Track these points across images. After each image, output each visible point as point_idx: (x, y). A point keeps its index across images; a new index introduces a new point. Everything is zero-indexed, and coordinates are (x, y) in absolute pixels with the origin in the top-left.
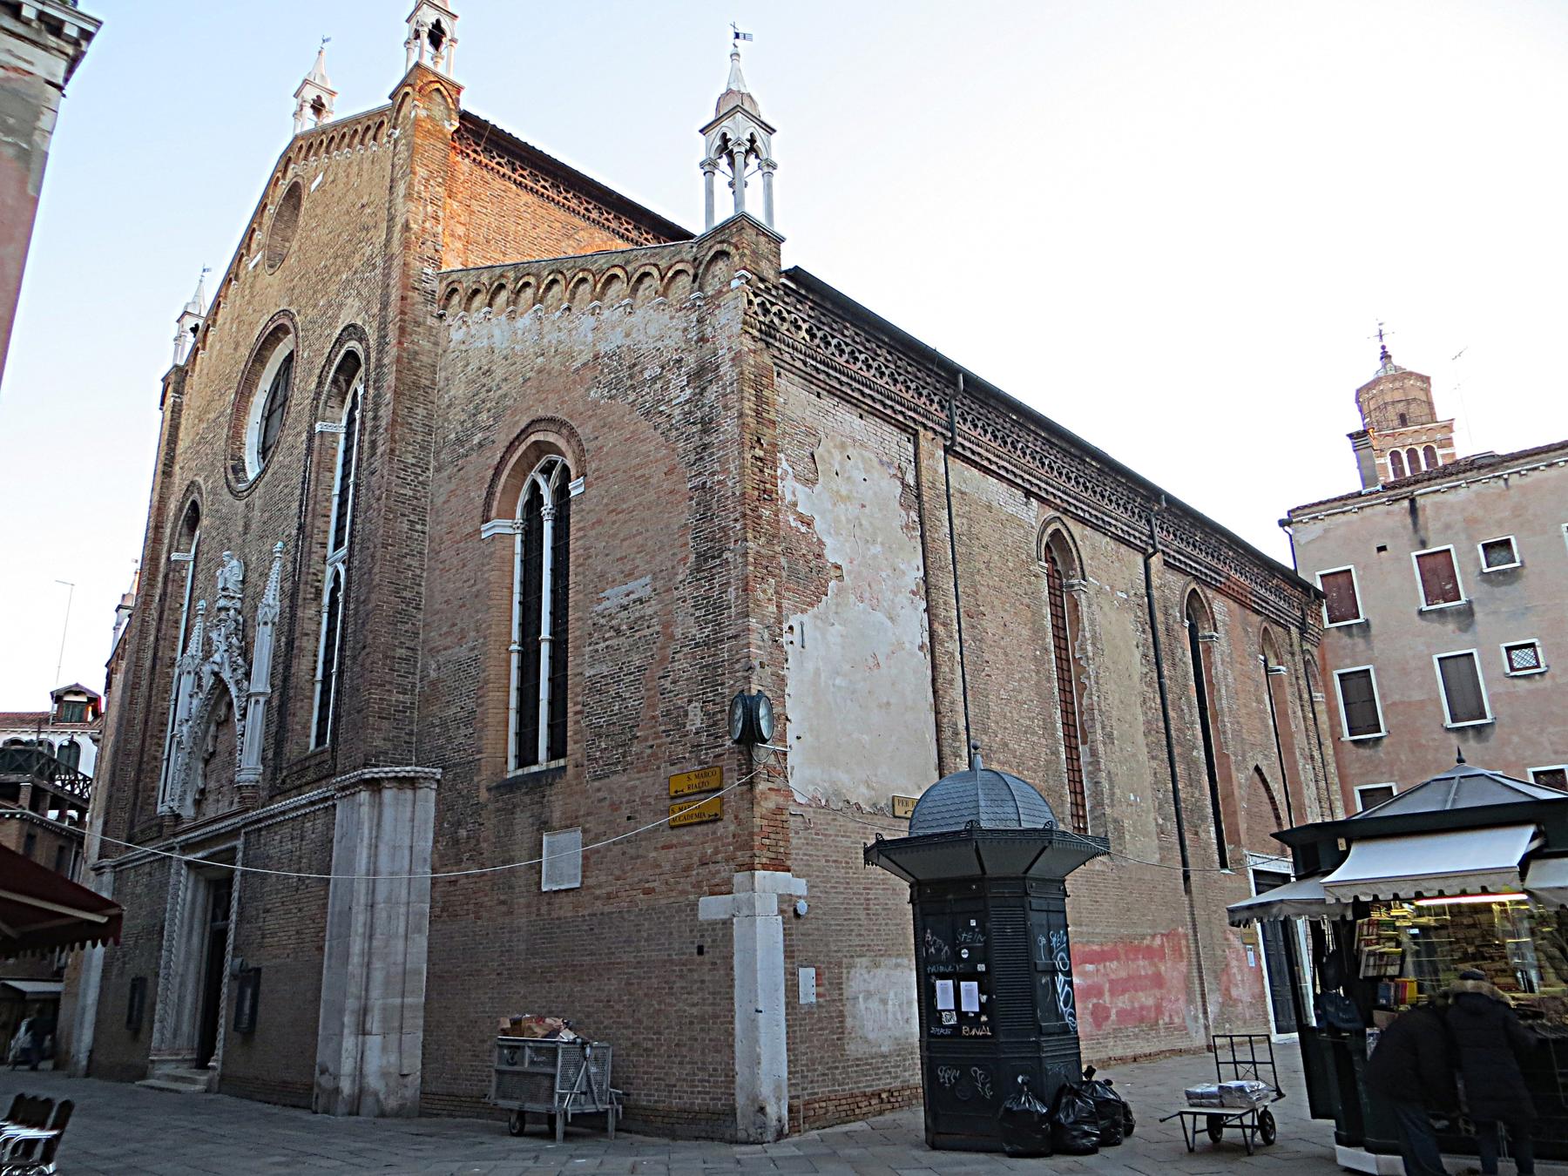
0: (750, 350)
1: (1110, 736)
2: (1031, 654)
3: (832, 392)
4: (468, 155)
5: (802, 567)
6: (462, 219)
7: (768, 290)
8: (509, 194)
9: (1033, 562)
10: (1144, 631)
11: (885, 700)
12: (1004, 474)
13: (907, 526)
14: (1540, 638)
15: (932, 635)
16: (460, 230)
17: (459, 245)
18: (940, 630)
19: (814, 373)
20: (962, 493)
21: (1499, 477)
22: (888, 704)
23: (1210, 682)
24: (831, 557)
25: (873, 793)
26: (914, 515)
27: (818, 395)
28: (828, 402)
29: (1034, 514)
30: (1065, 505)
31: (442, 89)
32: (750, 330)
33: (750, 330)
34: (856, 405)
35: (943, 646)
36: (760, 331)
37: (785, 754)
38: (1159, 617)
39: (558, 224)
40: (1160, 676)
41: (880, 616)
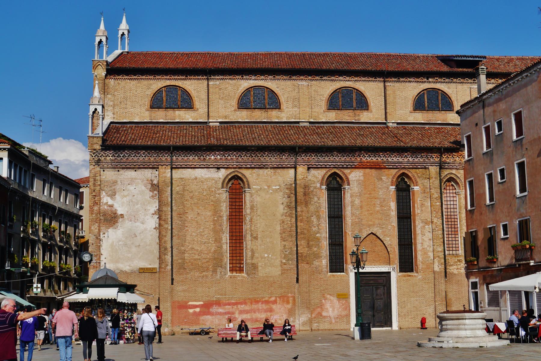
0: (93, 169)
1: (256, 238)
2: (211, 220)
3: (123, 168)
4: (112, 78)
5: (109, 218)
6: (112, 100)
7: (97, 152)
8: (127, 84)
9: (219, 189)
10: (289, 197)
11: (138, 245)
12: (203, 166)
13: (152, 196)
14: (506, 167)
15: (160, 225)
16: (111, 103)
17: (111, 108)
18: (162, 223)
19: (115, 166)
20: (181, 178)
21: (500, 90)
22: (139, 245)
23: (344, 205)
24: (119, 213)
25: (131, 268)
26: (156, 192)
27: (118, 171)
28: (122, 171)
29: (223, 173)
30: (239, 166)
31: (100, 64)
32: (92, 164)
33: (92, 164)
34: (133, 168)
35: (163, 227)
36: (95, 163)
37: (100, 263)
38: (300, 191)
39: (145, 86)
40: (296, 211)
41: (138, 224)
